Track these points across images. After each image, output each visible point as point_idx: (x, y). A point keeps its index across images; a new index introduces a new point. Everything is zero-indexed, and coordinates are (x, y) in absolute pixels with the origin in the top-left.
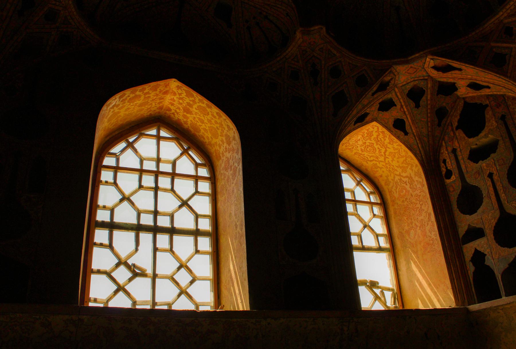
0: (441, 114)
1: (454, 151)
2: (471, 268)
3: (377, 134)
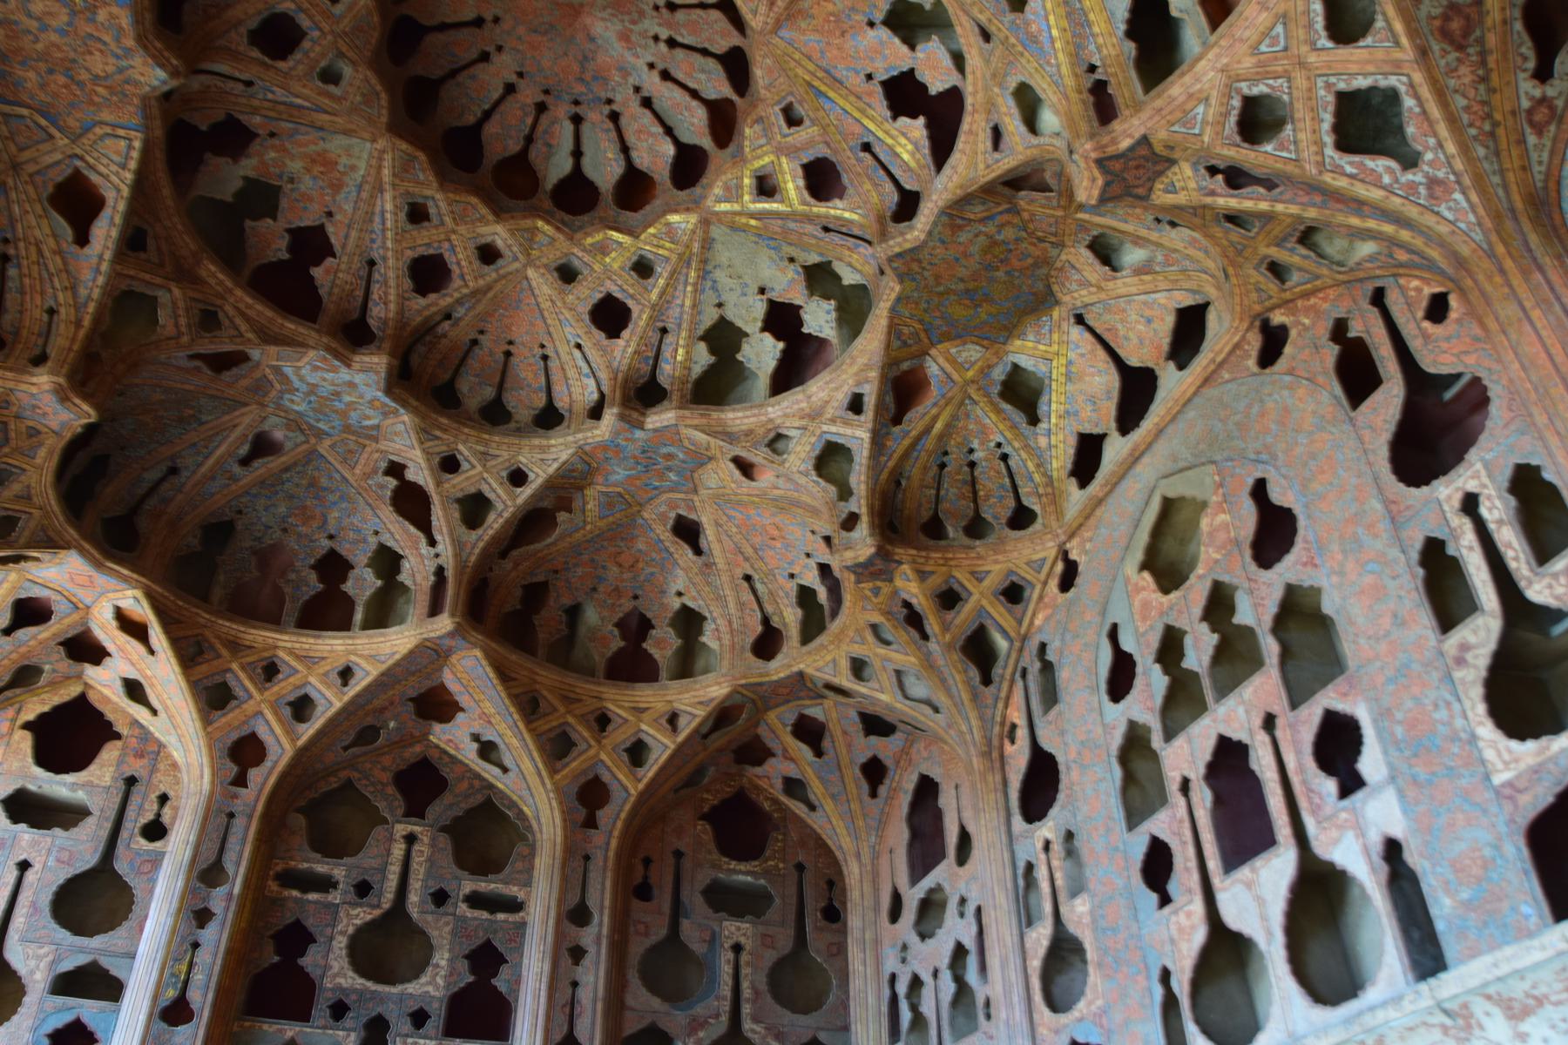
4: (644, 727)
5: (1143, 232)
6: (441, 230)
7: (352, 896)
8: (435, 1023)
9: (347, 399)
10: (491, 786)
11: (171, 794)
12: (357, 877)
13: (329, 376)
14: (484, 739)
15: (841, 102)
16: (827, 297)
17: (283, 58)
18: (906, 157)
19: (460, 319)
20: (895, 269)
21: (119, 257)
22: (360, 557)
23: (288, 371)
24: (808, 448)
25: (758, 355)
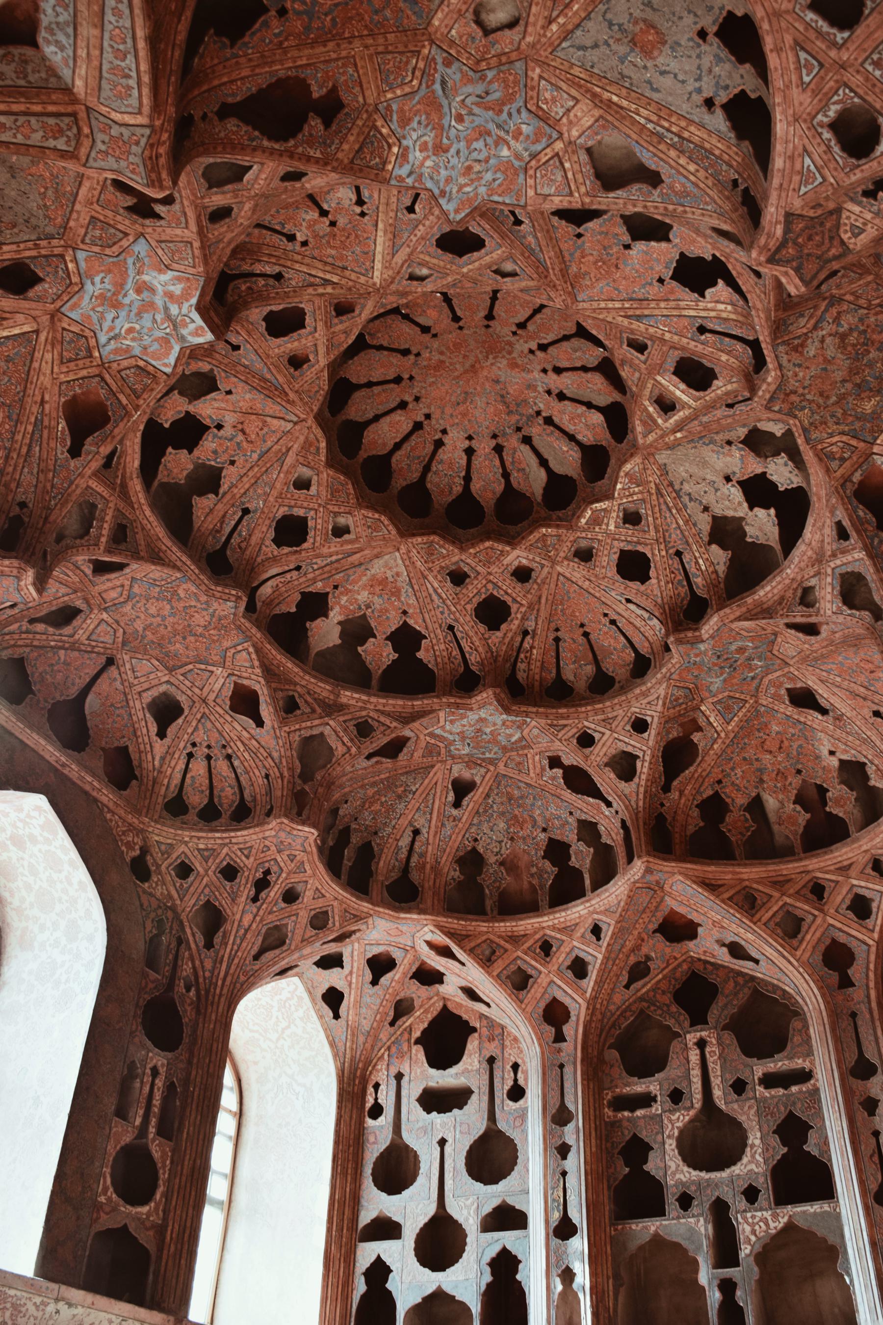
0: (402, 1009)
1: (399, 1077)
2: (361, 1286)
3: (289, 995)
4: (855, 882)
6: (480, 578)
7: (669, 1104)
8: (766, 1196)
9: (488, 730)
10: (753, 978)
11: (520, 1062)
12: (668, 1088)
13: (465, 722)
14: (727, 942)
15: (657, 312)
16: (776, 454)
17: (305, 540)
19: (534, 631)
20: (779, 412)
21: (283, 722)
22: (570, 835)
23: (438, 732)
24: (829, 589)
25: (761, 529)
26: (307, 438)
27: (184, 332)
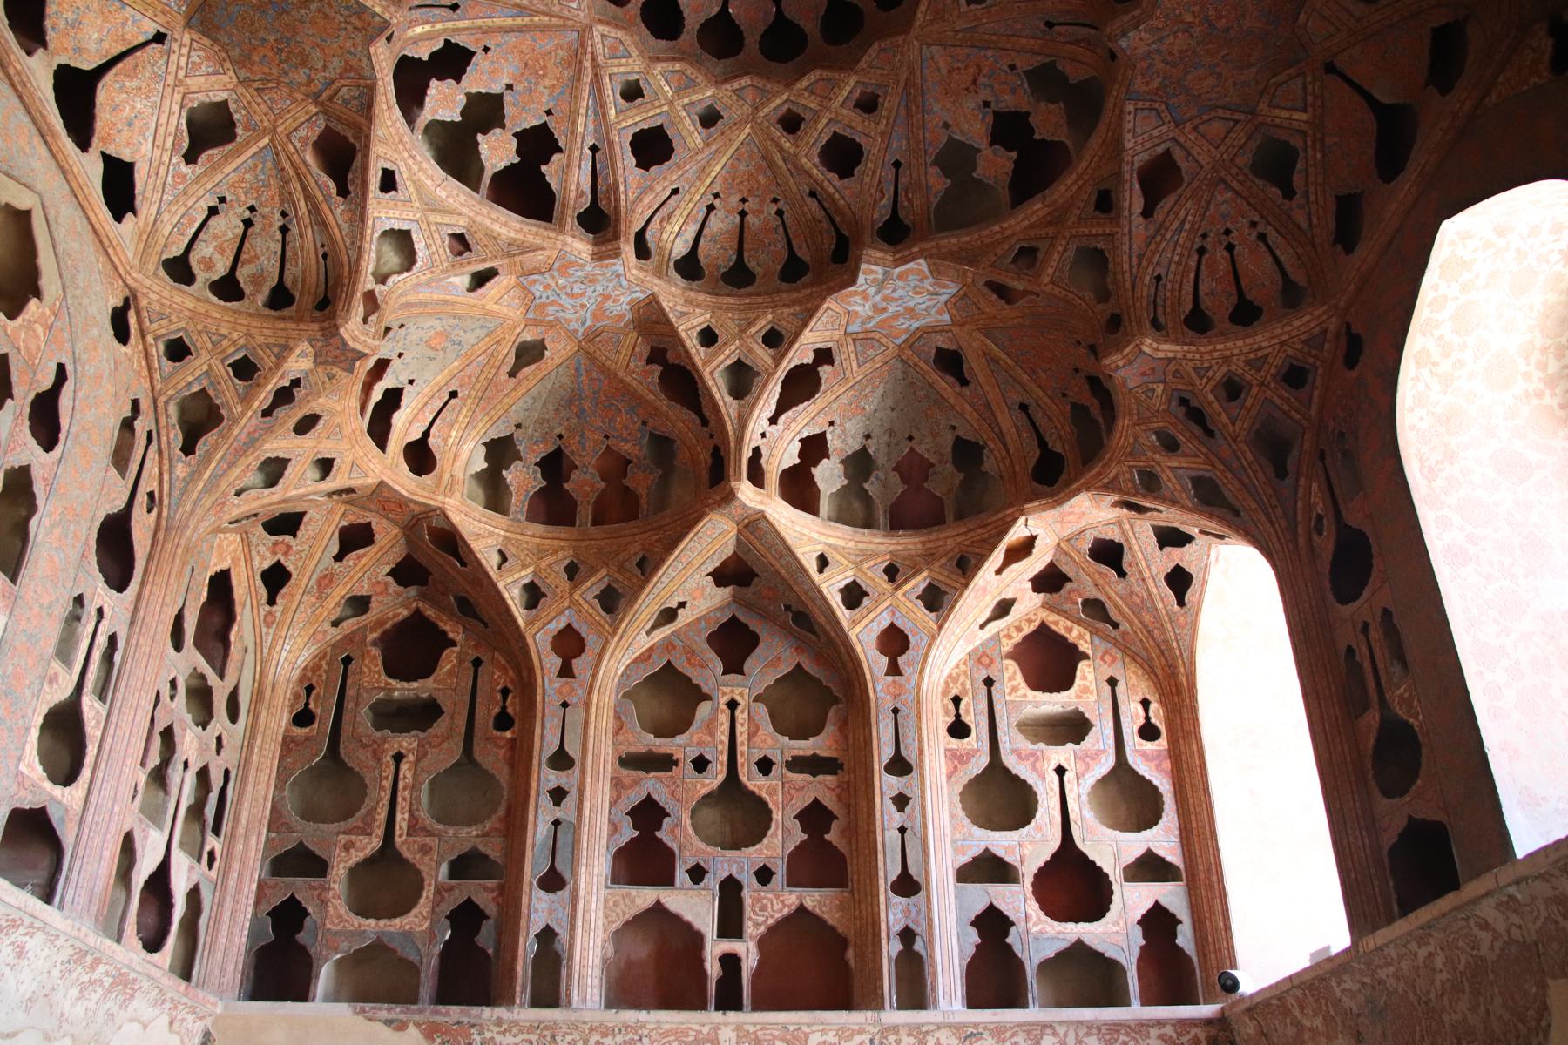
5: (219, 177)
18: (419, 30)
20: (375, 14)
26: (931, 23)
27: (880, 276)
